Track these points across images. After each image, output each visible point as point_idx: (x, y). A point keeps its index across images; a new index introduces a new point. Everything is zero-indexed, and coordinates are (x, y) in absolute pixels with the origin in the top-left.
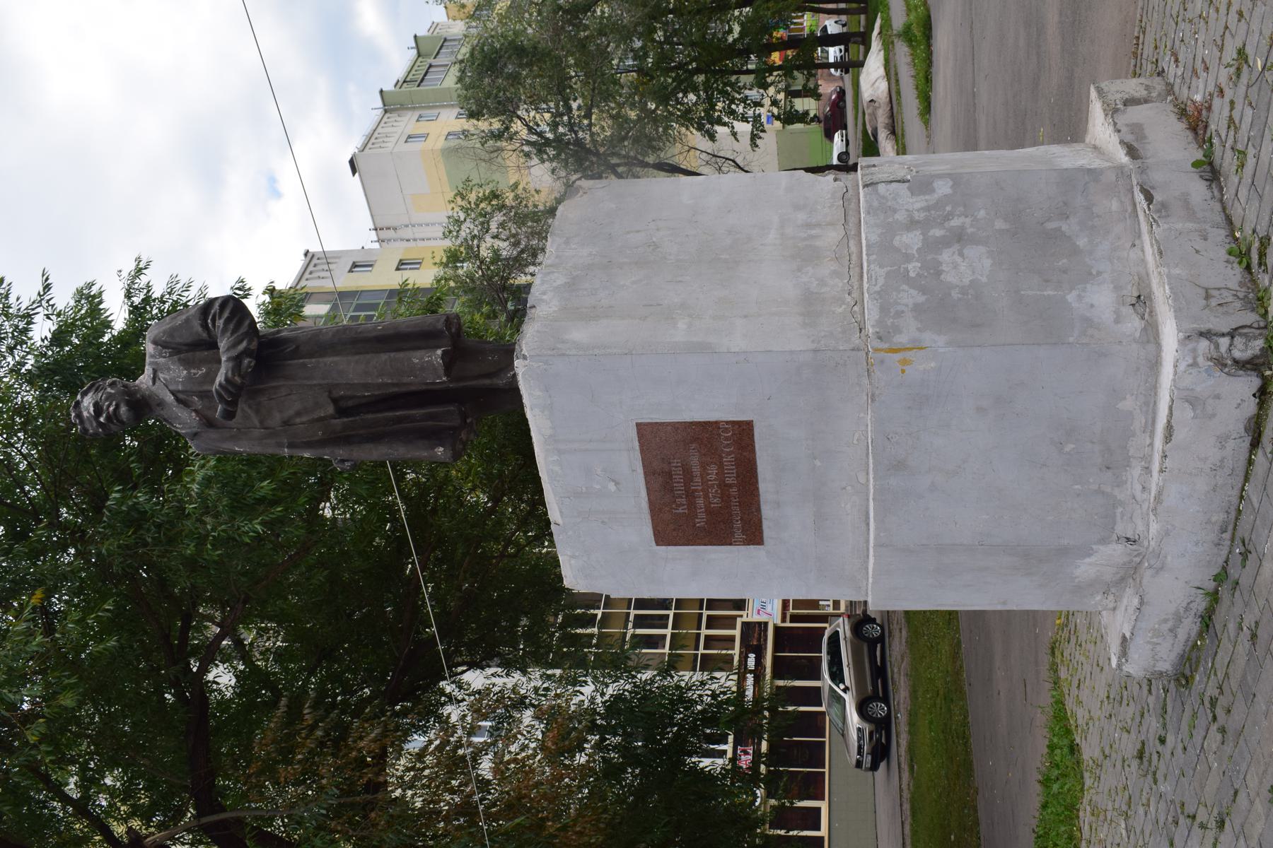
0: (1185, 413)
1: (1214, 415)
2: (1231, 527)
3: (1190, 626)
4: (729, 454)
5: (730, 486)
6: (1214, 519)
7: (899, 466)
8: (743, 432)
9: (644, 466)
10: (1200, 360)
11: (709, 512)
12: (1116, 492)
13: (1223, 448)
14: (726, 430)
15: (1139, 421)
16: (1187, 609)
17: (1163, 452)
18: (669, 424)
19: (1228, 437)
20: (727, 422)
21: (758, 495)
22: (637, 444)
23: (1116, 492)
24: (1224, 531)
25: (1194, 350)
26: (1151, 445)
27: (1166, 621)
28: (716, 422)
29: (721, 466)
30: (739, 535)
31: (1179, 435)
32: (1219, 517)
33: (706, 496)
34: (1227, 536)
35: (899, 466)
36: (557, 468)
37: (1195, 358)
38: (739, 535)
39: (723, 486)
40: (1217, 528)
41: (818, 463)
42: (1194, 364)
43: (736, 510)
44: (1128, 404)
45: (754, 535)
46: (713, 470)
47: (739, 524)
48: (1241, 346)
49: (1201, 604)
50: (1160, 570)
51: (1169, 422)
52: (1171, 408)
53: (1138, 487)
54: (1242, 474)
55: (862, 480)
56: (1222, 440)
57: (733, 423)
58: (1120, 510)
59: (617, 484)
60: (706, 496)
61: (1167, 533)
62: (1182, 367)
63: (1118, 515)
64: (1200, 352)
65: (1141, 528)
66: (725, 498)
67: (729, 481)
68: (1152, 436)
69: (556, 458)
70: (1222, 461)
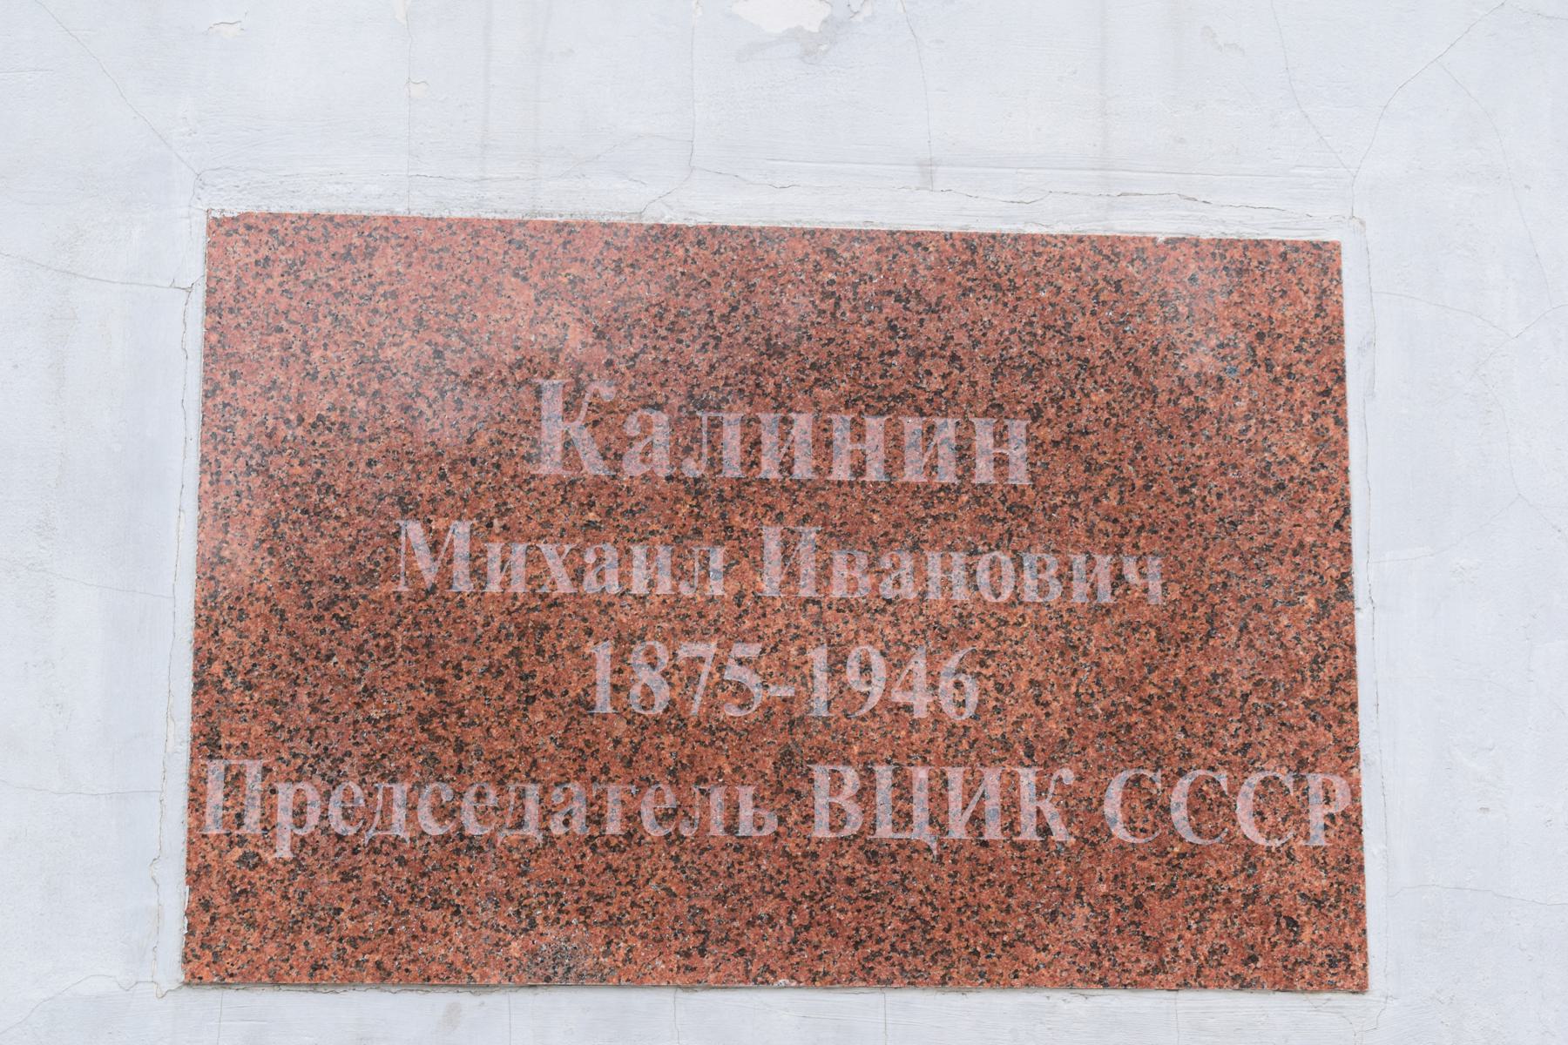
4: (1082, 809)
5: (787, 786)
9: (971, 244)
11: (535, 625)
14: (1281, 807)
18: (1331, 451)
20: (1350, 824)
28: (1348, 752)
29: (963, 744)
30: (291, 813)
33: (687, 619)
38: (291, 813)
39: (788, 754)
43: (548, 813)
46: (938, 689)
47: (409, 813)
57: (1346, 865)
60: (687, 619)
66: (681, 747)
67: (831, 794)
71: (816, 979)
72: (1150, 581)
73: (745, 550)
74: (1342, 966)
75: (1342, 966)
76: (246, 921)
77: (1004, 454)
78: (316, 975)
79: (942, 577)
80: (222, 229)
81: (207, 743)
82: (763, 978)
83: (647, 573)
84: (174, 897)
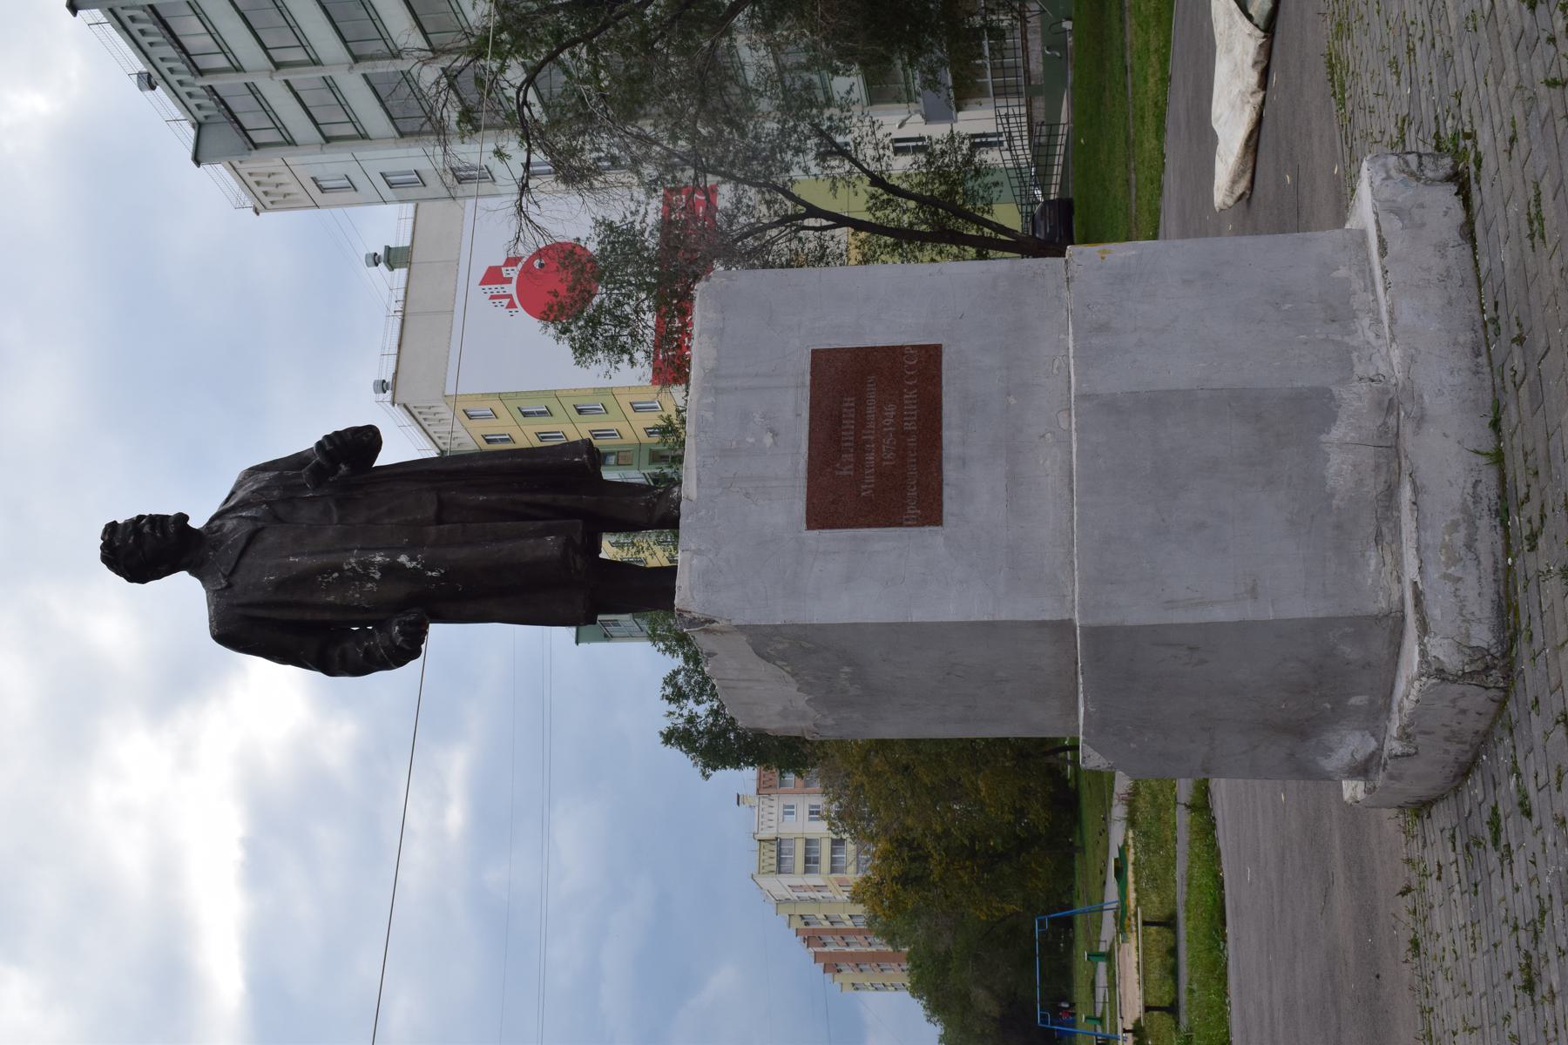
0: (1393, 225)
1: (1423, 225)
2: (1484, 350)
3: (1488, 538)
4: (911, 388)
5: (908, 434)
6: (1461, 339)
7: (1102, 328)
8: (930, 356)
9: (811, 408)
10: (1393, 173)
12: (1347, 339)
13: (1443, 256)
15: (1357, 285)
16: (1476, 499)
17: (1383, 268)
18: (849, 350)
19: (1445, 245)
20: (913, 347)
21: (940, 447)
22: (808, 377)
23: (1347, 339)
24: (1478, 355)
25: (1384, 165)
26: (1376, 300)
27: (1455, 526)
30: (913, 510)
31: (1394, 247)
32: (1466, 337)
34: (1483, 360)
35: (1102, 328)
36: (709, 415)
37: (1387, 172)
38: (913, 510)
40: (1468, 350)
41: (1012, 400)
42: (1388, 177)
44: (1342, 272)
45: (931, 514)
46: (890, 411)
48: (1430, 166)
49: (1489, 490)
50: (1420, 420)
51: (1379, 236)
52: (1377, 222)
53: (1371, 336)
54: (1474, 285)
55: (1064, 426)
56: (1441, 249)
58: (1355, 354)
59: (775, 434)
61: (1413, 359)
62: (1377, 181)
63: (1355, 360)
64: (1391, 166)
65: (1383, 369)
67: (908, 426)
68: (1374, 292)
69: (710, 399)
70: (1448, 270)
71: (940, 428)
72: (871, 378)
73: (867, 442)
74: (937, 349)
75: (937, 349)
76: (931, 514)
77: (850, 402)
78: (940, 505)
79: (871, 411)
80: (809, 527)
81: (901, 525)
82: (940, 437)
83: (871, 457)
84: (927, 529)
